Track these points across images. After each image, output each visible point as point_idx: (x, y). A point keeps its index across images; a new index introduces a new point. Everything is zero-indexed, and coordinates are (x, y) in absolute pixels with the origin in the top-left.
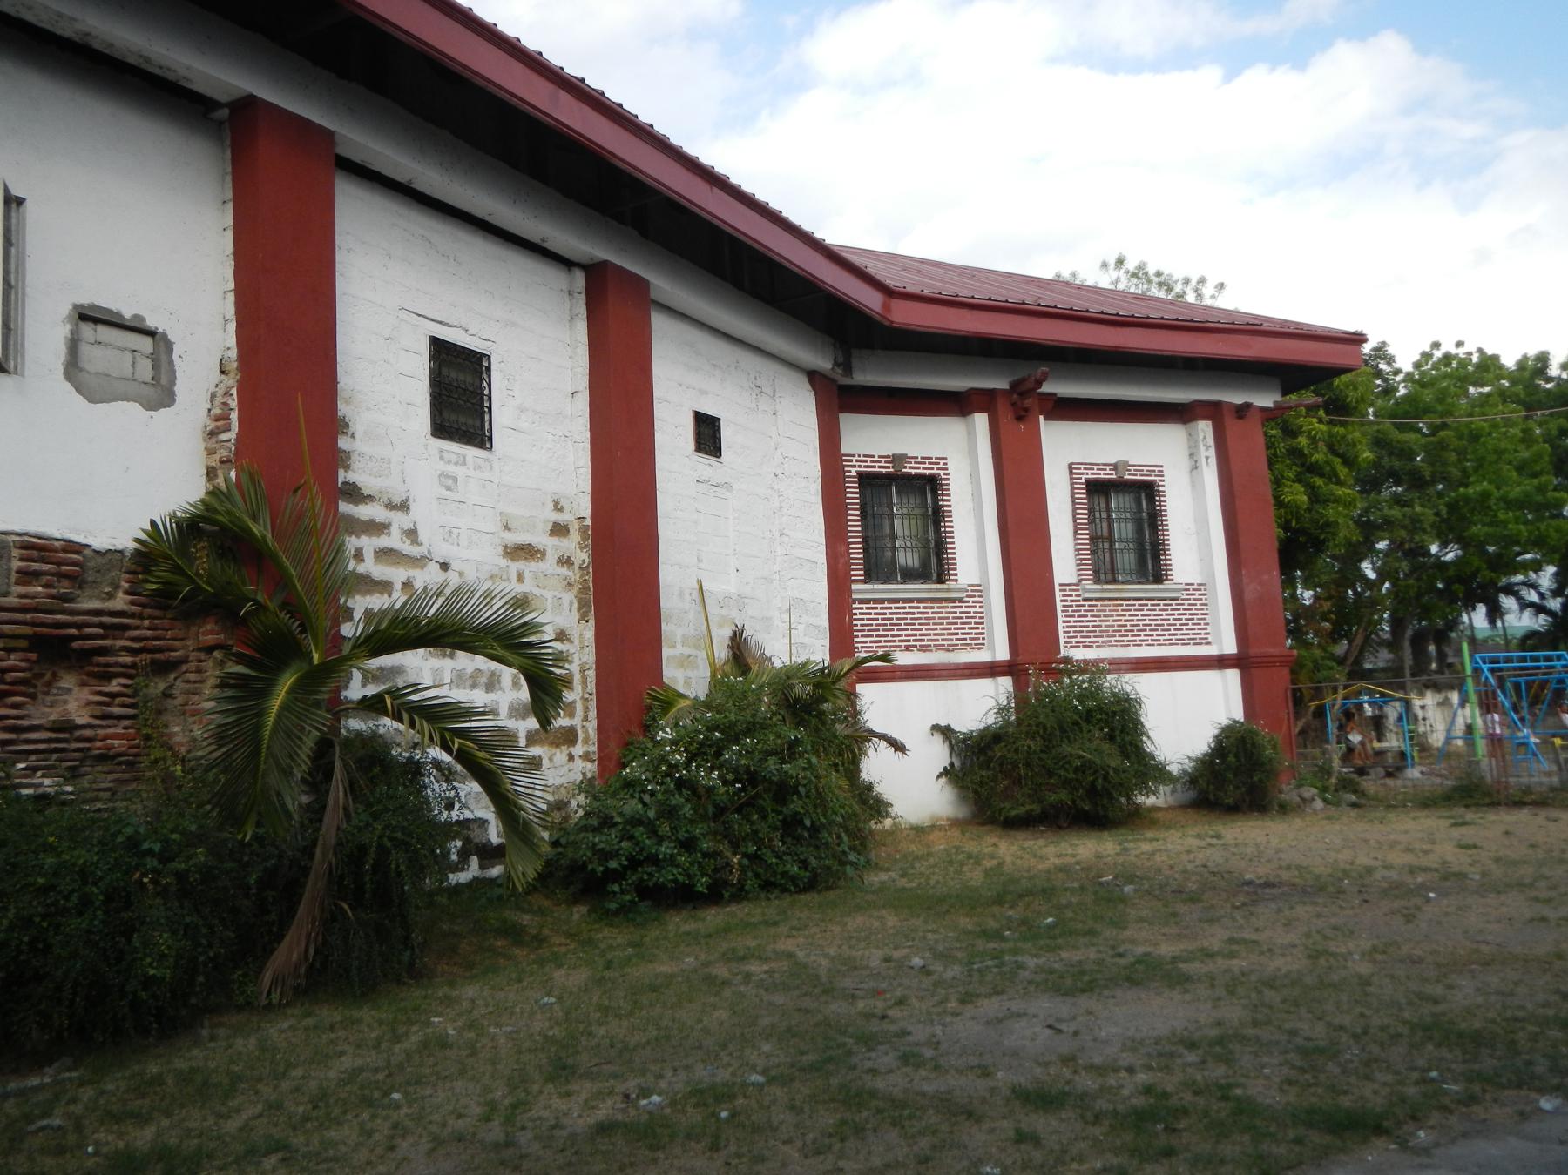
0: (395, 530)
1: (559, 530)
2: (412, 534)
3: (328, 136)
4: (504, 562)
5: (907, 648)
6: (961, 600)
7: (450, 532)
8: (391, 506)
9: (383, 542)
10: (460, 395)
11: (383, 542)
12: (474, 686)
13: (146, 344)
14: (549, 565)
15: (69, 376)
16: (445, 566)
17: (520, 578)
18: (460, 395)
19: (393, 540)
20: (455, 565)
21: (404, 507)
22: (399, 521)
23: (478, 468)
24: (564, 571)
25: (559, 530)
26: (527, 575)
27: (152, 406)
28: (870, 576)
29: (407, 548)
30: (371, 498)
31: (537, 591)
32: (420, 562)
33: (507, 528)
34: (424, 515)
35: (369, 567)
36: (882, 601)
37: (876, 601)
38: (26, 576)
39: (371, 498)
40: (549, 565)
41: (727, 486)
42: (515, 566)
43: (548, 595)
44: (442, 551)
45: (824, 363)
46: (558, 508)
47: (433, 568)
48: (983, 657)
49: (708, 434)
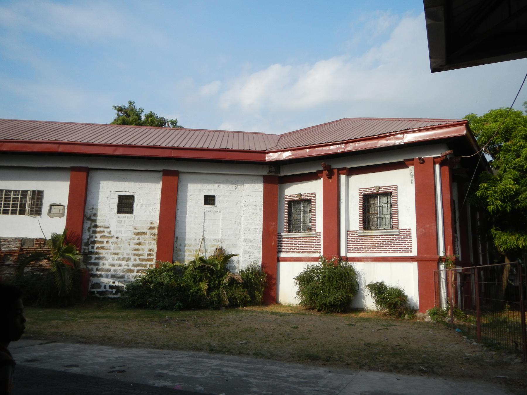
0: (106, 232)
1: (151, 228)
2: (110, 233)
3: (87, 167)
4: (134, 236)
5: (299, 252)
6: (316, 237)
7: (119, 232)
8: (105, 228)
9: (103, 234)
10: (125, 205)
11: (103, 234)
12: (123, 260)
13: (62, 207)
14: (148, 236)
15: (48, 215)
16: (117, 238)
17: (138, 239)
18: (125, 205)
19: (105, 234)
20: (120, 237)
21: (108, 227)
22: (107, 230)
23: (128, 218)
24: (153, 237)
25: (151, 228)
26: (141, 238)
27: (60, 217)
28: (289, 231)
29: (108, 235)
30: (100, 227)
31: (143, 241)
32: (111, 237)
33: (136, 229)
34: (113, 229)
35: (98, 239)
36: (292, 238)
37: (290, 238)
38: (37, 244)
39: (100, 227)
40: (148, 236)
41: (220, 212)
42: (137, 237)
43: (147, 242)
44: (117, 235)
45: (265, 173)
46: (152, 223)
47: (115, 238)
48: (317, 255)
49: (209, 200)
